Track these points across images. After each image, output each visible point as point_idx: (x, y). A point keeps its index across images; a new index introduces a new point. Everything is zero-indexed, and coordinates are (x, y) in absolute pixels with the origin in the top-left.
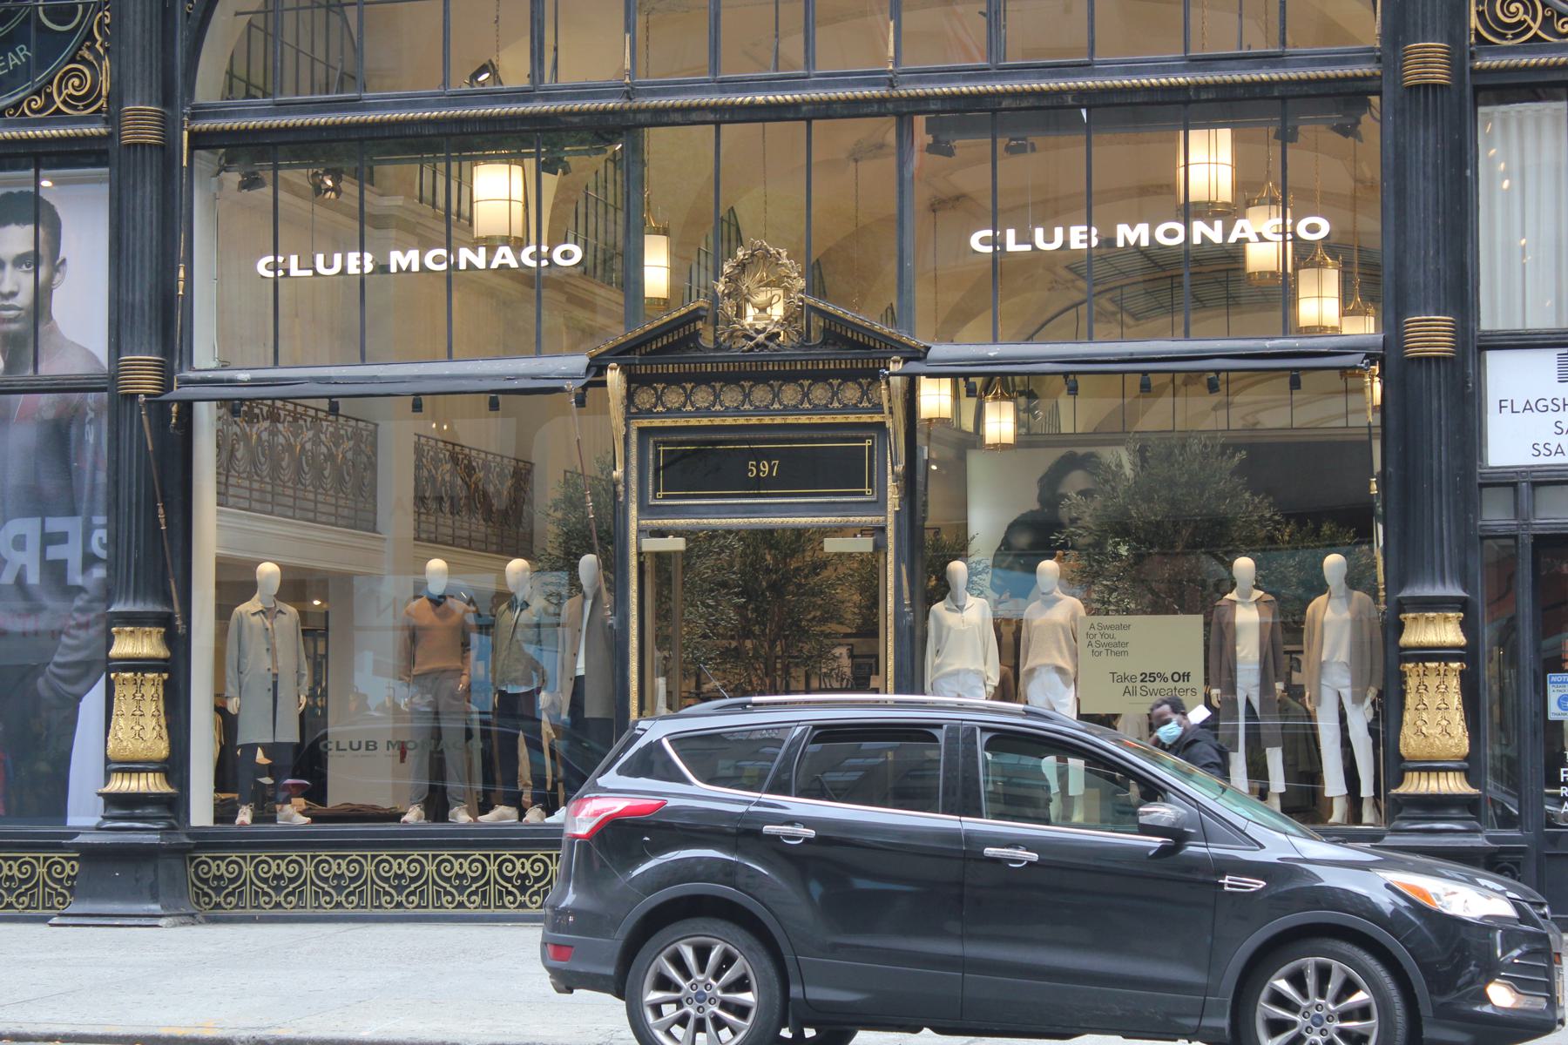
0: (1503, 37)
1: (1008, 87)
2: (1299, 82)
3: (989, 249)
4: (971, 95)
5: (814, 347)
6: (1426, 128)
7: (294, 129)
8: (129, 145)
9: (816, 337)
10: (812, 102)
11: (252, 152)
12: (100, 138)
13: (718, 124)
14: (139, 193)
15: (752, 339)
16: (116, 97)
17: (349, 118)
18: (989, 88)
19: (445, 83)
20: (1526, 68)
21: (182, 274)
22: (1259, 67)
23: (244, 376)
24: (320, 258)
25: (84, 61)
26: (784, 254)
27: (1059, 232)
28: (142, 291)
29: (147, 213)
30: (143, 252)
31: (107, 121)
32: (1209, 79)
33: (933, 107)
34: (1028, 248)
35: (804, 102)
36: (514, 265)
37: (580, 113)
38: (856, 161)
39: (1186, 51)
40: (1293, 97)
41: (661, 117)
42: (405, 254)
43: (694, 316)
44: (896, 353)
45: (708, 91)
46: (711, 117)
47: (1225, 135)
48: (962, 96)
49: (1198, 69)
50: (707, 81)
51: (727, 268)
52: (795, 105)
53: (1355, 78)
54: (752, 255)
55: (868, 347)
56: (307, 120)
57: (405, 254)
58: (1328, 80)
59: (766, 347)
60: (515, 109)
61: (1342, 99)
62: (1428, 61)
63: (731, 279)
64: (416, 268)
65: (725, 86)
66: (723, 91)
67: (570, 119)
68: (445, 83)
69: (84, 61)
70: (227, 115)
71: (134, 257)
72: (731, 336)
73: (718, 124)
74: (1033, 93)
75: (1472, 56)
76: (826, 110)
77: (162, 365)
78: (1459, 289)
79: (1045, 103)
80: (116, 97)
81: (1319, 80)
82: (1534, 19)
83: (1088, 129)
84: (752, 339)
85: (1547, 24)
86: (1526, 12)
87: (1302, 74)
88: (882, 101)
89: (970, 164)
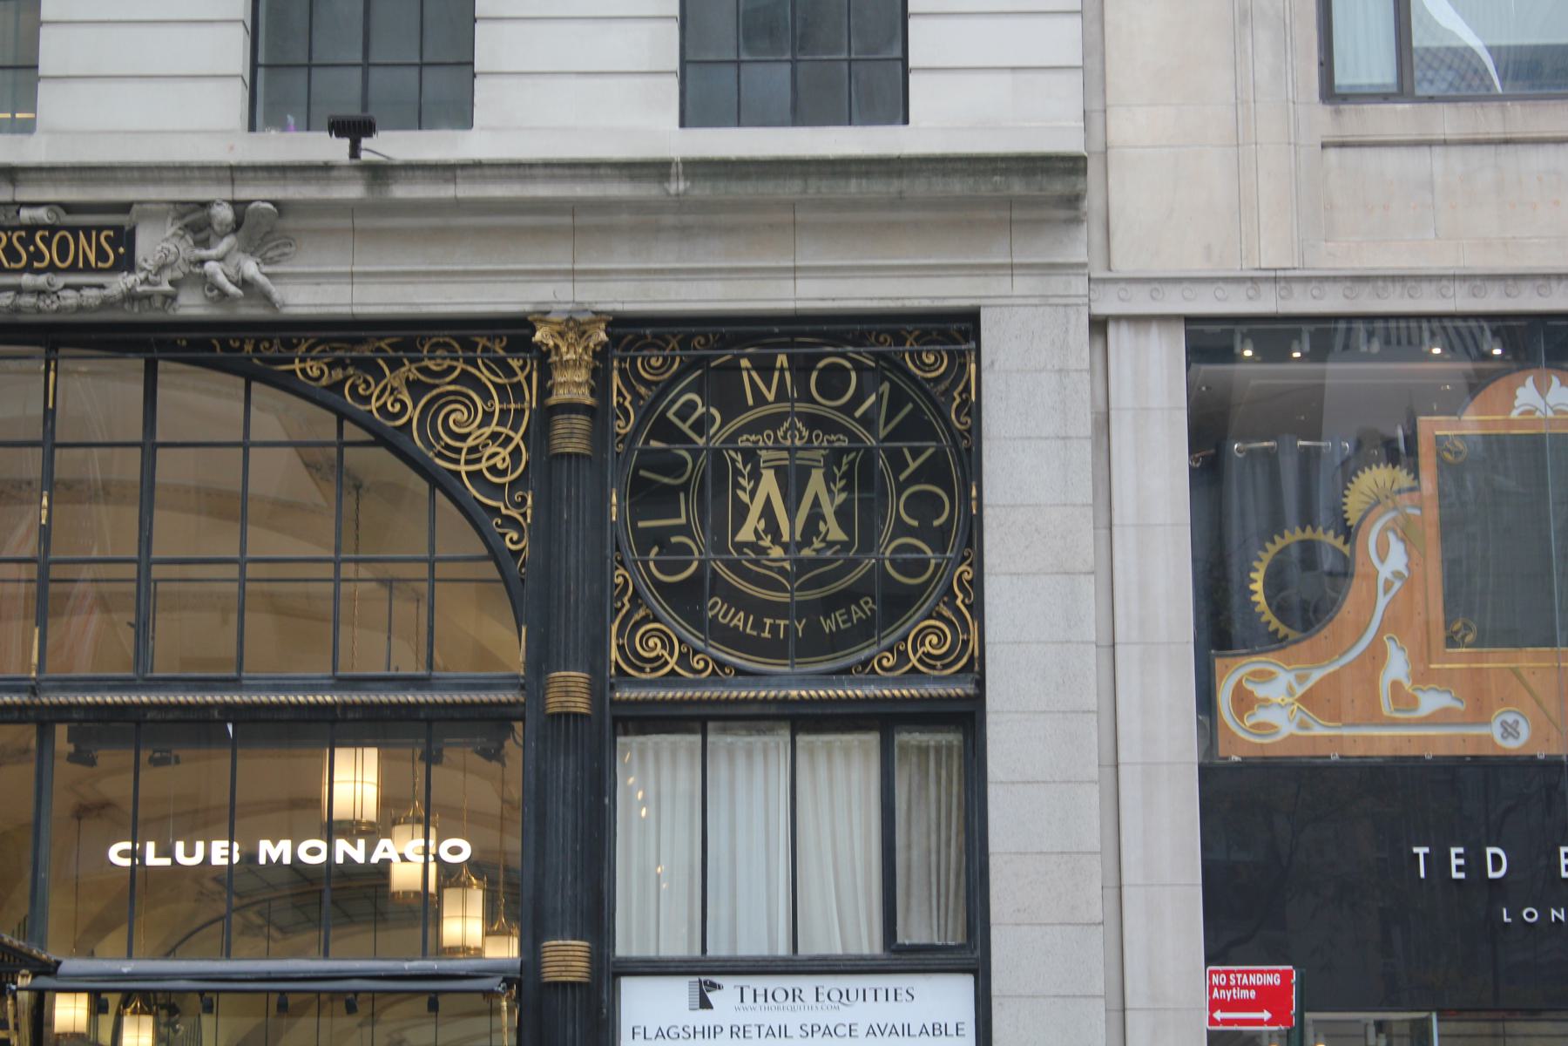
0: (642, 670)
2: (445, 705)
3: (127, 862)
4: (115, 706)
6: (567, 755)
20: (664, 701)
27: (200, 846)
33: (75, 716)
34: (167, 862)
39: (335, 668)
44: (25, 967)
47: (371, 754)
48: (106, 706)
53: (500, 704)
58: (473, 704)
61: (484, 724)
62: (570, 690)
74: (179, 706)
75: (612, 687)
78: (595, 916)
81: (464, 705)
82: (671, 654)
83: (234, 744)
85: (684, 660)
86: (664, 647)
87: (448, 697)
88: (22, 708)
89: (113, 773)
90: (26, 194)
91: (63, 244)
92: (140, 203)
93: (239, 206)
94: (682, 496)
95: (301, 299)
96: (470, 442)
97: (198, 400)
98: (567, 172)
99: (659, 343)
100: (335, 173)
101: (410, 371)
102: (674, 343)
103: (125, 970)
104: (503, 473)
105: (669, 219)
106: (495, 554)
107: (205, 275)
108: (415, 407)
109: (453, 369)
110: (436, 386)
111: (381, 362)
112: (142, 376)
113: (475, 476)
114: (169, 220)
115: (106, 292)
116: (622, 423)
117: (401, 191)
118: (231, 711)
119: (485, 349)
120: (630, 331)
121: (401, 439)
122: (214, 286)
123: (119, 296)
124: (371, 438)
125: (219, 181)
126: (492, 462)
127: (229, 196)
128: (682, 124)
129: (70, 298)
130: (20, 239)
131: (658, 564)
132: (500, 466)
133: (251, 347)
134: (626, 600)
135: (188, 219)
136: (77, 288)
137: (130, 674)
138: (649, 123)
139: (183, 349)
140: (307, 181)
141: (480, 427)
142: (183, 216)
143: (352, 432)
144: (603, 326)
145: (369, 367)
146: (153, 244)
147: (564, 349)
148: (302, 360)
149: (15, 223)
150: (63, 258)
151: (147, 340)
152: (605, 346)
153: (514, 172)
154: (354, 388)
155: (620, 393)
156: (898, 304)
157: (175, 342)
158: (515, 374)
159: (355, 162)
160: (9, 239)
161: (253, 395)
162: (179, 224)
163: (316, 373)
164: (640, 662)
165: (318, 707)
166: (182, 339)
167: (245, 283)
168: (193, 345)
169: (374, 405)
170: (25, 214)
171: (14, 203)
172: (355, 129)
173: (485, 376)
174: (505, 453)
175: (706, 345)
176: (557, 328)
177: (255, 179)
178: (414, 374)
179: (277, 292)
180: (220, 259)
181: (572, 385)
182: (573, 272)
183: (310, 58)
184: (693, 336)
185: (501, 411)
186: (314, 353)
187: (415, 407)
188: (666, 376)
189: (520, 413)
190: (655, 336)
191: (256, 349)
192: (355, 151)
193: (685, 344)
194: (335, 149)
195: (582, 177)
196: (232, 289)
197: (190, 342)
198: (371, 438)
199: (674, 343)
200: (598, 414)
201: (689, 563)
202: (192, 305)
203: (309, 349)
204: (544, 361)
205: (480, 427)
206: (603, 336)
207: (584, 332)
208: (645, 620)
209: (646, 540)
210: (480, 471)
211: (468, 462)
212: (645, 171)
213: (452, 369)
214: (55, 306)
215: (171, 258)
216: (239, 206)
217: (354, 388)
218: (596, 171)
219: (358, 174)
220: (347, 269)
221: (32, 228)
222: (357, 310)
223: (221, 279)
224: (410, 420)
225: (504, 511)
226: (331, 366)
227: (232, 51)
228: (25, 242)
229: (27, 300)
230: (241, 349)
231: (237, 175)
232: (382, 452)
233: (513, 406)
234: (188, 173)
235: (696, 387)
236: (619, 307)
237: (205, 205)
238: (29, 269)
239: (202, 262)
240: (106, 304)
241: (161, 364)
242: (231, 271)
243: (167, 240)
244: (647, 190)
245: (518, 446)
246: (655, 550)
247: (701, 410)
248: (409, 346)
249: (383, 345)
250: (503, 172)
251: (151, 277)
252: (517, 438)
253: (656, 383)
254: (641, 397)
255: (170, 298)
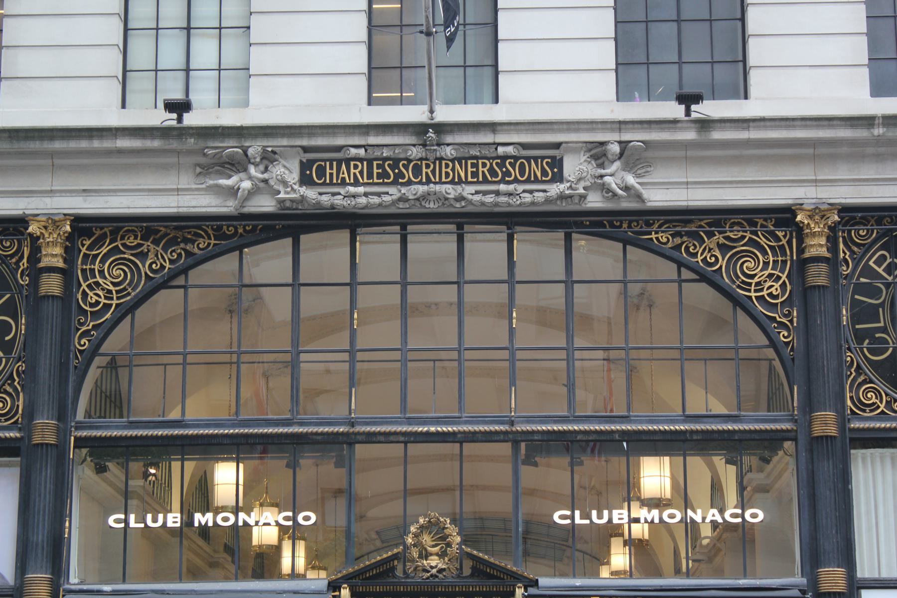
0: (864, 411)
1: (581, 428)
2: (750, 431)
3: (290, 523)
4: (559, 432)
5: (466, 577)
6: (828, 459)
7: (142, 437)
8: (38, 444)
9: (467, 571)
10: (464, 432)
11: (102, 451)
12: (16, 439)
13: (406, 443)
14: (44, 474)
15: (428, 572)
16: (30, 413)
17: (176, 432)
18: (570, 428)
19: (237, 413)
20: (879, 429)
21: (67, 524)
22: (726, 422)
23: (107, 588)
24: (149, 517)
25: (6, 392)
26: (448, 521)
27: (606, 512)
28: (41, 536)
29: (48, 486)
30: (44, 512)
31: (20, 430)
32: (699, 428)
33: (536, 438)
34: (588, 522)
35: (459, 432)
36: (720, 520)
37: (322, 434)
38: (317, 465)
39: (684, 410)
40: (746, 440)
41: (371, 438)
42: (204, 515)
43: (395, 557)
44: (520, 582)
45: (400, 424)
46: (402, 439)
47: (667, 459)
48: (554, 432)
49: (691, 422)
50: (399, 418)
51: (413, 529)
52: (454, 434)
53: (782, 431)
54: (429, 521)
55: (497, 578)
56: (150, 432)
57: (204, 515)
58: (766, 431)
59: (437, 577)
60: (281, 430)
61: (767, 443)
62: (825, 423)
63: (416, 536)
64: (657, 521)
65: (410, 421)
66: (410, 424)
67: (315, 437)
68: (237, 413)
69: (6, 392)
70: (91, 428)
71: (39, 512)
72: (415, 569)
73: (406, 443)
74: (596, 432)
76: (472, 437)
77: (51, 580)
79: (603, 438)
80: (30, 413)
81: (761, 431)
82: (881, 402)
83: (627, 454)
84: (428, 572)
86: (877, 398)
87: (752, 427)
88: (506, 433)
90: (500, 138)
91: (522, 166)
92: (567, 143)
93: (623, 144)
94: (881, 310)
95: (658, 198)
96: (756, 280)
97: (596, 257)
98: (814, 123)
99: (864, 221)
100: (679, 125)
101: (719, 238)
102: (872, 222)
103: (578, 584)
104: (776, 297)
105: (870, 150)
106: (773, 344)
107: (604, 184)
108: (723, 259)
109: (744, 237)
110: (735, 247)
111: (702, 234)
112: (563, 243)
113: (760, 299)
114: (582, 153)
115: (548, 194)
116: (845, 268)
117: (717, 135)
118: (626, 435)
119: (762, 226)
120: (852, 215)
121: (716, 278)
122: (609, 190)
123: (555, 197)
124: (698, 277)
125: (612, 130)
126: (770, 291)
127: (618, 139)
128: (618, 100)
129: (528, 198)
130: (497, 163)
131: (869, 349)
132: (775, 293)
133: (627, 225)
134: (853, 370)
135: (593, 152)
136: (531, 192)
137: (566, 414)
138: (852, 95)
139: (586, 227)
140: (662, 130)
141: (761, 271)
142: (590, 150)
143: (686, 274)
144: (836, 212)
145: (695, 235)
146: (575, 166)
147: (812, 226)
148: (656, 233)
149: (494, 155)
150: (522, 175)
151: (566, 221)
152: (837, 224)
153: (783, 123)
154: (687, 248)
155: (844, 252)
156: (665, 204)
157: (582, 222)
158: (781, 241)
159: (687, 118)
160: (491, 164)
161: (628, 256)
162: (588, 155)
163: (665, 240)
164: (862, 406)
165: (676, 432)
166: (586, 220)
167: (627, 188)
168: (593, 224)
169: (699, 258)
170: (501, 150)
171: (494, 144)
172: (688, 99)
173: (763, 241)
174: (777, 285)
175: (891, 223)
176: (808, 213)
177: (634, 129)
178: (722, 241)
179: (646, 194)
180: (611, 175)
181: (817, 246)
182: (816, 181)
183: (648, 59)
184: (885, 217)
185: (774, 261)
186: (663, 229)
187: (723, 259)
188: (869, 241)
189: (784, 262)
190: (861, 218)
191: (629, 227)
192: (688, 113)
193: (879, 222)
194: (676, 111)
195: (823, 126)
196: (620, 192)
197: (590, 221)
198: (698, 277)
199: (872, 222)
200: (833, 262)
201: (887, 349)
202: (595, 201)
203: (660, 227)
204: (800, 231)
205: (761, 271)
206: (836, 218)
207: (824, 216)
208: (865, 382)
209: (860, 336)
210: (763, 296)
211: (756, 291)
212: (860, 122)
213: (743, 237)
214: (518, 202)
215: (585, 174)
216: (623, 144)
217: (687, 248)
218: (831, 123)
219: (693, 125)
220: (685, 180)
221: (504, 158)
222: (691, 203)
223: (614, 186)
224: (721, 267)
225: (778, 319)
226: (673, 236)
227: (606, 55)
228: (501, 165)
229: (503, 199)
230: (621, 226)
231: (623, 126)
232: (704, 285)
233: (780, 259)
234: (594, 126)
235: (882, 248)
236: (843, 201)
237: (602, 144)
238: (503, 181)
239: (602, 176)
240: (548, 201)
241: (574, 236)
242: (619, 182)
243: (581, 164)
244: (860, 133)
245: (784, 281)
246: (867, 341)
247: (889, 260)
248: (717, 224)
249: (702, 223)
250: (777, 123)
251: (573, 185)
252: (784, 277)
253: (864, 245)
254: (854, 253)
255: (583, 197)
